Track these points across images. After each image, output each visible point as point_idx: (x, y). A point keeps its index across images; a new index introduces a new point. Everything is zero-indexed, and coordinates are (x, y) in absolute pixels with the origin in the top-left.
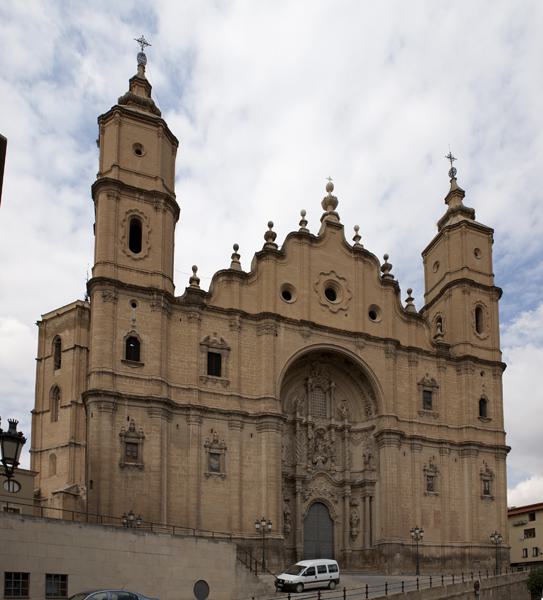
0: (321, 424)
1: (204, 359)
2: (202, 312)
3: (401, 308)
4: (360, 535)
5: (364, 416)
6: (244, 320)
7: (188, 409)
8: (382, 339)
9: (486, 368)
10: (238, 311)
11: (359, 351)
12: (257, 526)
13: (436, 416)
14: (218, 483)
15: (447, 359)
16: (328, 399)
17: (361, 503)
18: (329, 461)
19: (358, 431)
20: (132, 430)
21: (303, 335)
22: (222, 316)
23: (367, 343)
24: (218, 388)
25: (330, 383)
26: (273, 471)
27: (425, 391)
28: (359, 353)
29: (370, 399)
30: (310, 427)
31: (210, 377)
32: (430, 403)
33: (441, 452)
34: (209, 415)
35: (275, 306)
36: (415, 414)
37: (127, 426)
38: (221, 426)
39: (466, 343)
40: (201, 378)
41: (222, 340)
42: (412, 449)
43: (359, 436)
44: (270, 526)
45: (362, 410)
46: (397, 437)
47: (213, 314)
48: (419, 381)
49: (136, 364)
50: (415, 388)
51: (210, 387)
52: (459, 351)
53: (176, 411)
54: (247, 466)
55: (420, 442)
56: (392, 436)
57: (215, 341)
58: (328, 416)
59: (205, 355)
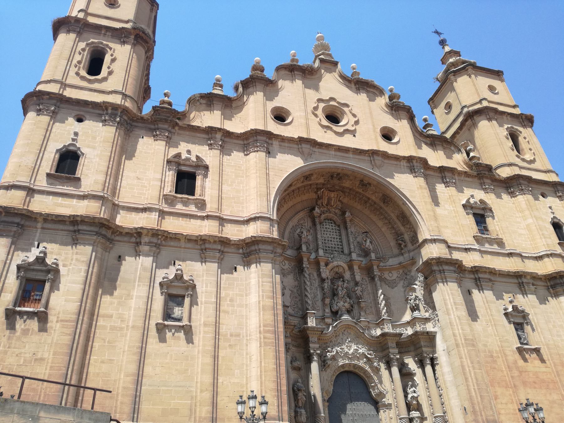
1: (171, 177)
2: (173, 130)
3: (421, 134)
5: (396, 251)
6: (226, 139)
8: (404, 158)
9: (544, 189)
10: (220, 129)
12: (240, 408)
13: (500, 243)
15: (492, 181)
16: (343, 232)
18: (356, 307)
19: (391, 269)
22: (198, 135)
23: (386, 161)
25: (344, 213)
26: (269, 317)
29: (402, 228)
30: (322, 264)
34: (172, 243)
35: (266, 124)
39: (510, 165)
40: (166, 198)
41: (198, 157)
43: (395, 275)
44: (264, 408)
45: (393, 243)
46: (452, 268)
47: (188, 133)
48: (464, 202)
49: (69, 179)
52: (504, 173)
53: (117, 238)
54: (227, 312)
55: (487, 276)
56: (446, 267)
58: (346, 251)
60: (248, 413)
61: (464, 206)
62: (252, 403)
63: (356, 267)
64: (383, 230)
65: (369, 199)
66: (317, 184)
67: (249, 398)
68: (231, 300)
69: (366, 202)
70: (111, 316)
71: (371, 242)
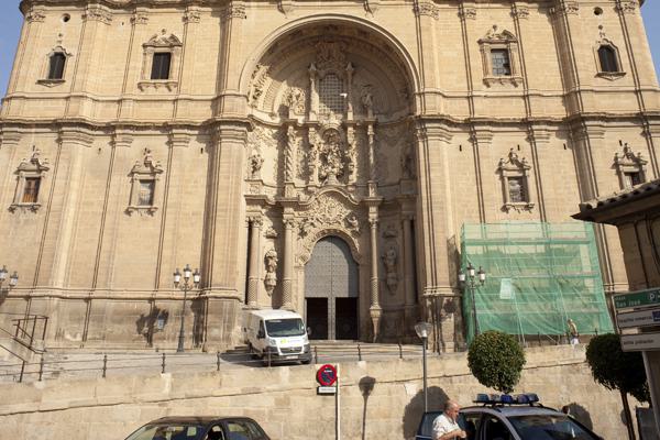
0: (334, 121)
4: (401, 282)
7: (114, 128)
11: (370, 14)
14: (146, 219)
17: (401, 232)
20: (34, 161)
21: (282, 11)
24: (162, 92)
27: (493, 51)
28: (370, 18)
31: (153, 81)
32: (507, 66)
33: (531, 139)
36: (477, 83)
37: (29, 155)
38: (158, 142)
41: (173, 37)
42: (473, 140)
50: (474, 48)
51: (151, 92)
57: (165, 40)
59: (150, 59)
60: (183, 283)
61: (480, 42)
62: (188, 274)
63: (350, 129)
64: (392, 79)
65: (372, 46)
66: (312, 38)
67: (185, 270)
68: (196, 182)
69: (371, 50)
70: (92, 204)
71: (372, 98)
